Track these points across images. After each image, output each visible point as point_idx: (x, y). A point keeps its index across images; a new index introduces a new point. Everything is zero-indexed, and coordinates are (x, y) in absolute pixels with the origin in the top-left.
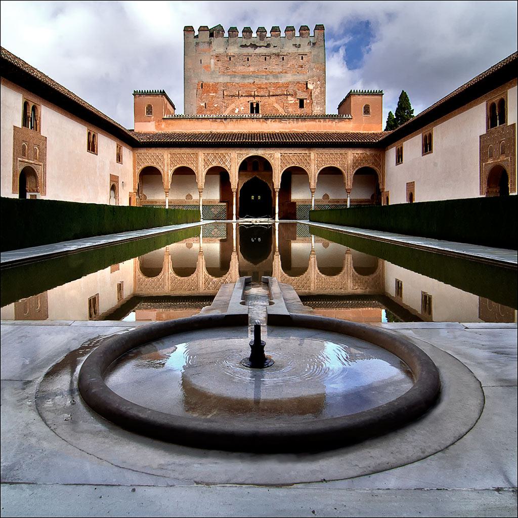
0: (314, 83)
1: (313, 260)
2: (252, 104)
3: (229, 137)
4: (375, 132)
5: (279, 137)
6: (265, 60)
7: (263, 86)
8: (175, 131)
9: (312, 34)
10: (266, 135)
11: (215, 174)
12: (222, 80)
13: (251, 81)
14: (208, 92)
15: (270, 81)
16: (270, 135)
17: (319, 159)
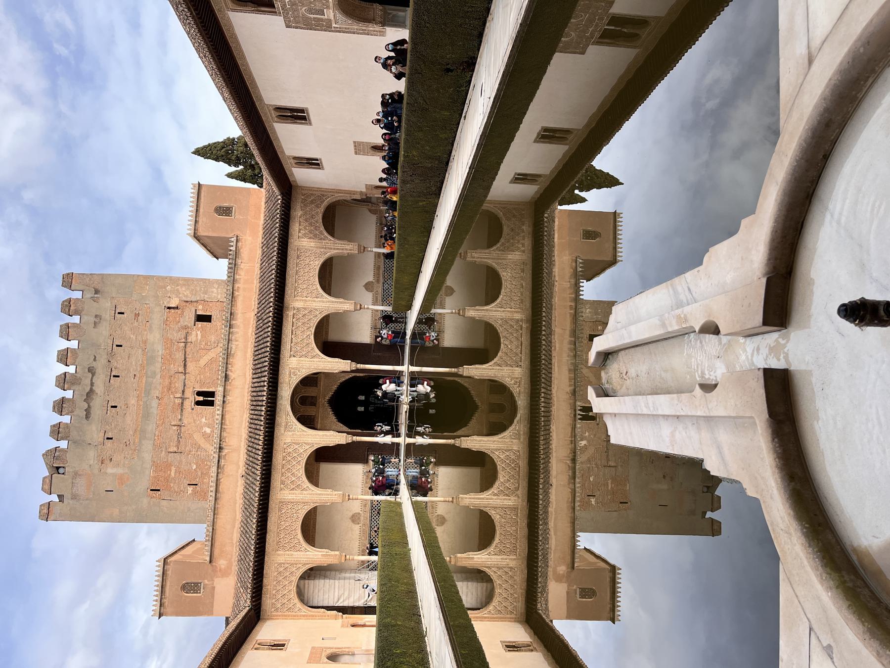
0: (169, 295)
1: (471, 313)
2: (198, 403)
3: (255, 446)
4: (264, 200)
5: (261, 358)
6: (118, 376)
7: (167, 381)
8: (234, 542)
9: (78, 295)
10: (255, 380)
11: (318, 472)
12: (147, 456)
13: (155, 403)
14: (167, 480)
15: (158, 370)
16: (255, 374)
17: (305, 294)
